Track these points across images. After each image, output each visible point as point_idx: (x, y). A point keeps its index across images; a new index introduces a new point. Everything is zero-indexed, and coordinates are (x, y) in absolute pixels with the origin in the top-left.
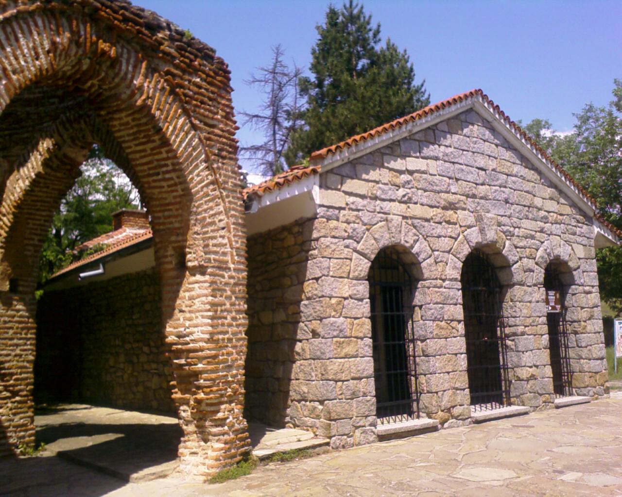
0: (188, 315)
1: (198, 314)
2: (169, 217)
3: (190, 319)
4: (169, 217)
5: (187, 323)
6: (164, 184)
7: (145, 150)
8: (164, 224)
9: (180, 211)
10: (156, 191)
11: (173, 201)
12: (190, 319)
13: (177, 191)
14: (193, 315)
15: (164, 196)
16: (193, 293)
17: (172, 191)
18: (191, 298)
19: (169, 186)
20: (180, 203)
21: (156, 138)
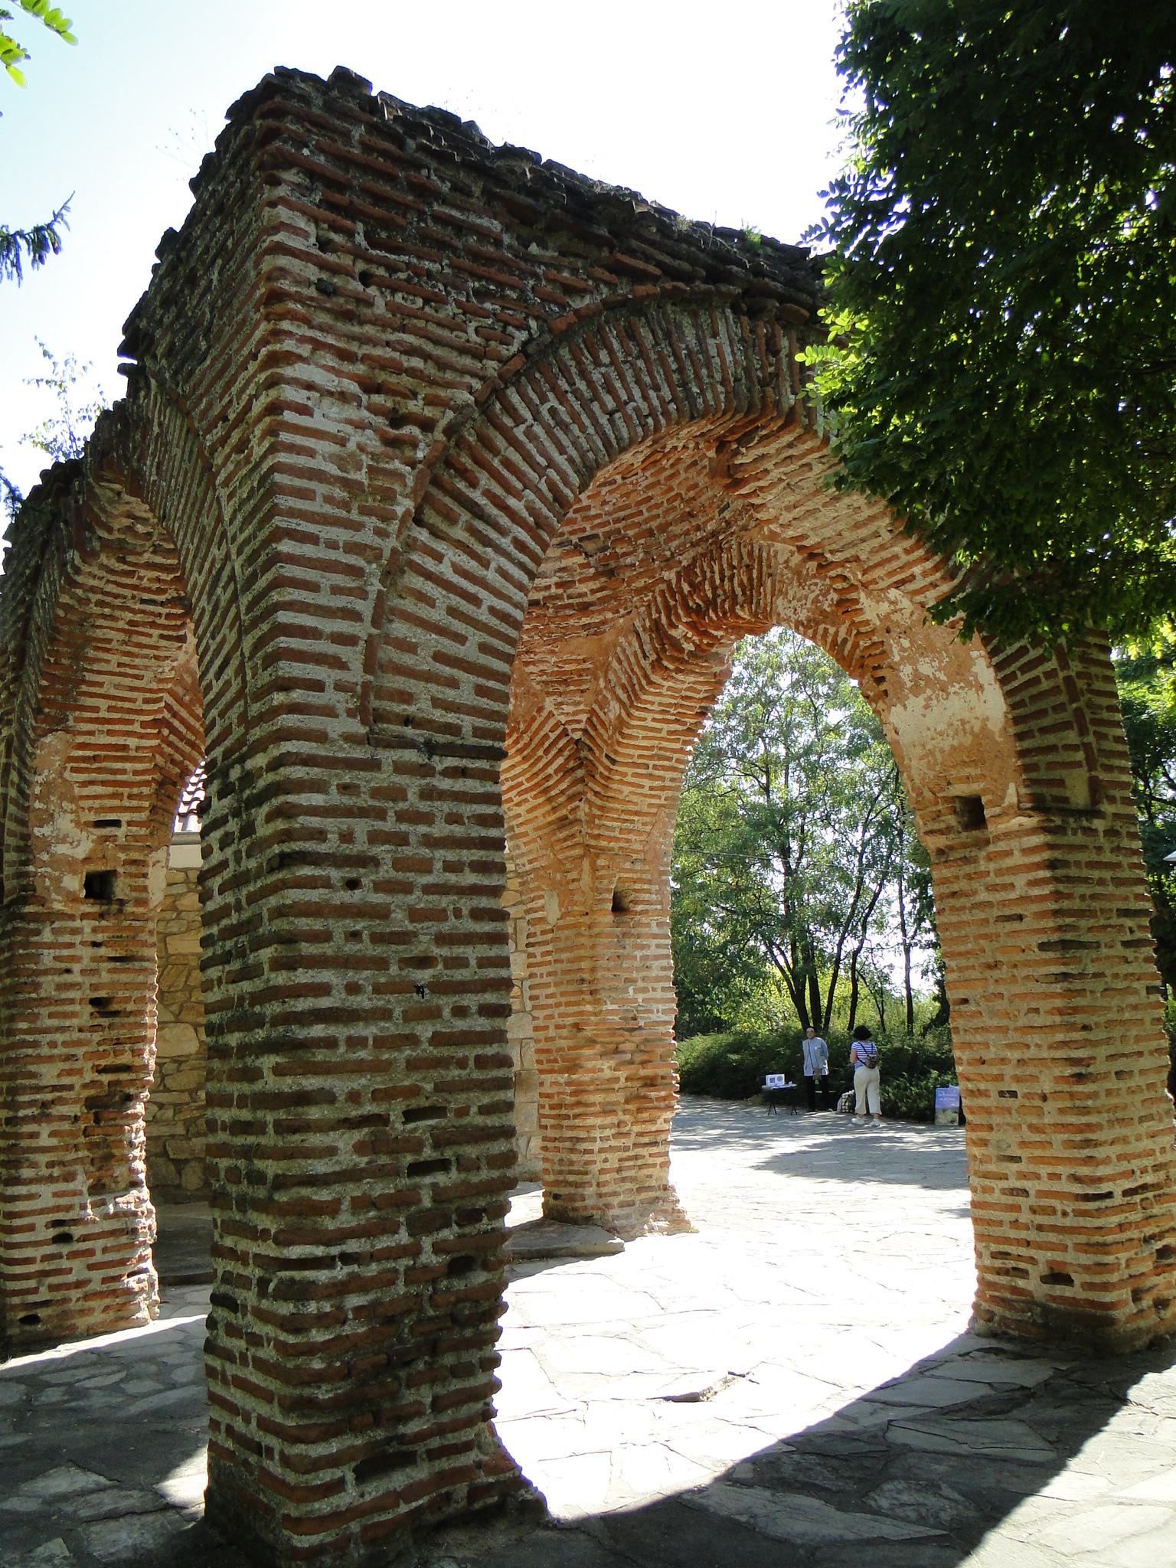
0: (640, 984)
1: (656, 985)
2: (630, 831)
3: (645, 990)
4: (630, 831)
5: (640, 997)
6: (647, 783)
7: (659, 731)
8: (617, 840)
9: (648, 828)
10: (626, 789)
11: (645, 809)
13: (660, 797)
14: (650, 986)
15: (635, 799)
16: (648, 953)
17: (652, 796)
18: (645, 958)
19: (651, 788)
20: (655, 814)
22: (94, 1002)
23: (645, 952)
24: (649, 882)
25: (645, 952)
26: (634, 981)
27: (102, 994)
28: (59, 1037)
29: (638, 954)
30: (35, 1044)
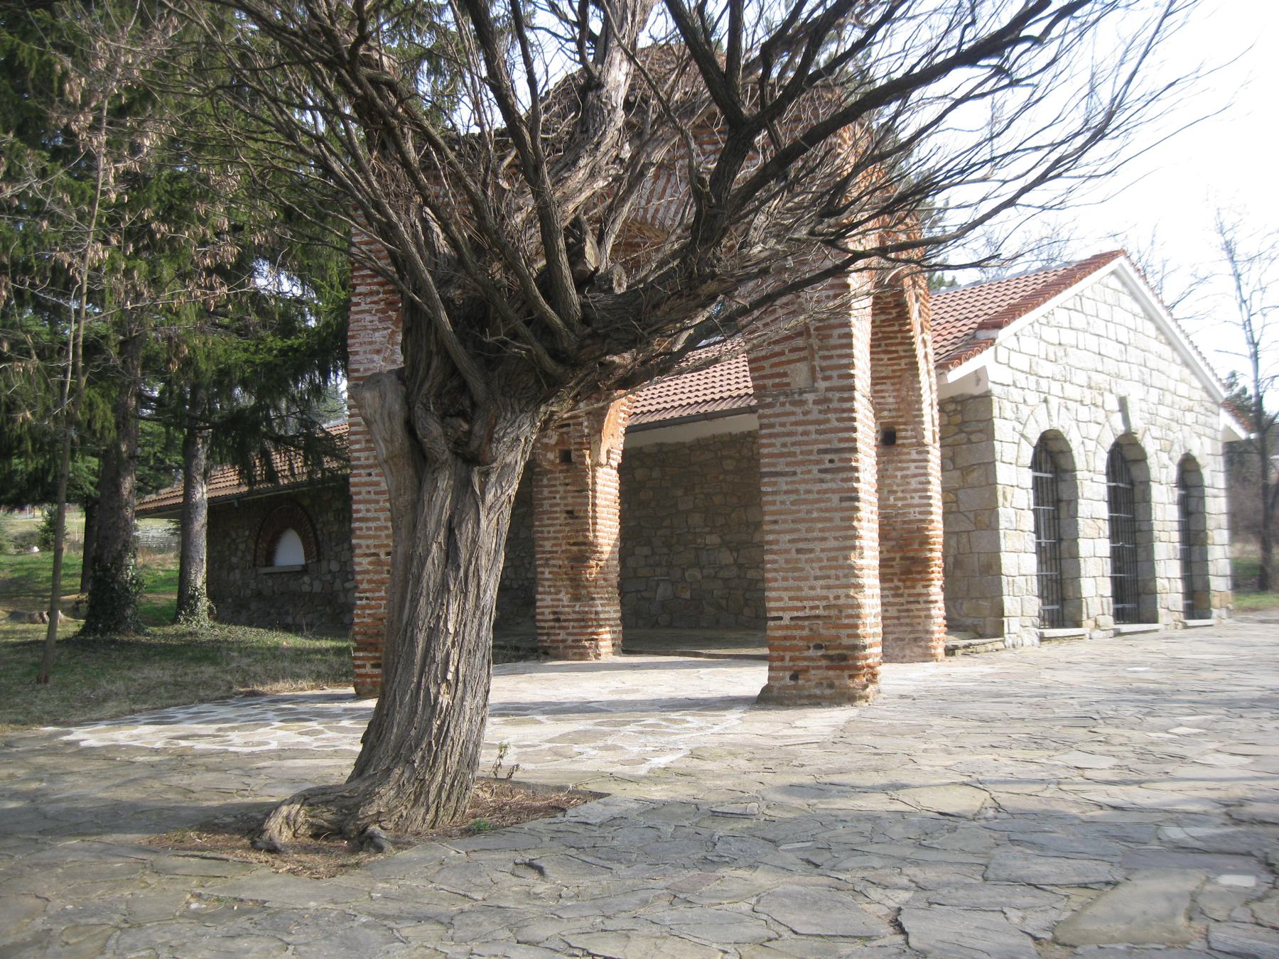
0: (900, 495)
2: (882, 391)
3: (904, 499)
5: (900, 504)
6: (885, 357)
12: (904, 499)
16: (908, 472)
18: (904, 477)
21: (894, 312)
22: (568, 512)
23: (905, 472)
24: (905, 424)
25: (905, 472)
26: (895, 492)
27: (570, 508)
28: (552, 529)
29: (899, 474)
30: (542, 532)
